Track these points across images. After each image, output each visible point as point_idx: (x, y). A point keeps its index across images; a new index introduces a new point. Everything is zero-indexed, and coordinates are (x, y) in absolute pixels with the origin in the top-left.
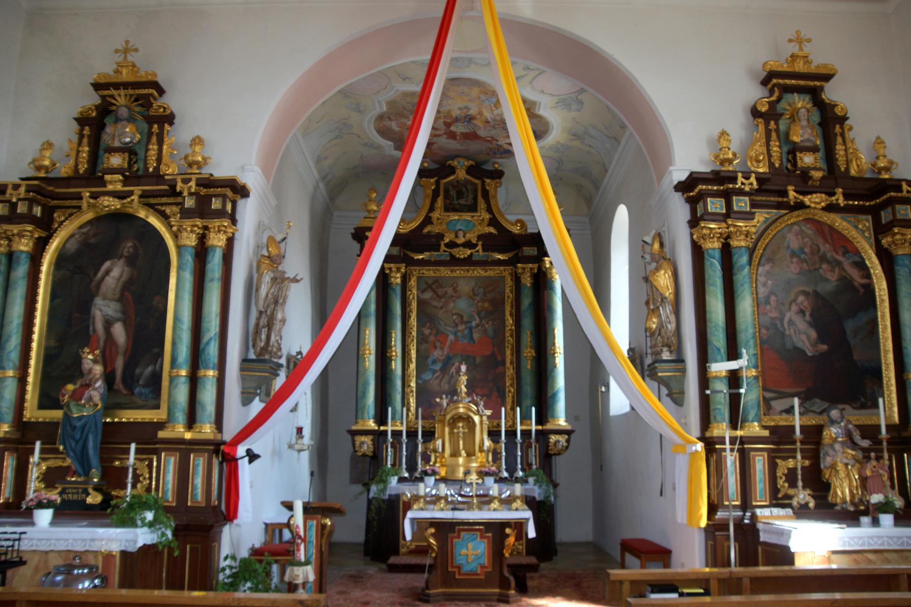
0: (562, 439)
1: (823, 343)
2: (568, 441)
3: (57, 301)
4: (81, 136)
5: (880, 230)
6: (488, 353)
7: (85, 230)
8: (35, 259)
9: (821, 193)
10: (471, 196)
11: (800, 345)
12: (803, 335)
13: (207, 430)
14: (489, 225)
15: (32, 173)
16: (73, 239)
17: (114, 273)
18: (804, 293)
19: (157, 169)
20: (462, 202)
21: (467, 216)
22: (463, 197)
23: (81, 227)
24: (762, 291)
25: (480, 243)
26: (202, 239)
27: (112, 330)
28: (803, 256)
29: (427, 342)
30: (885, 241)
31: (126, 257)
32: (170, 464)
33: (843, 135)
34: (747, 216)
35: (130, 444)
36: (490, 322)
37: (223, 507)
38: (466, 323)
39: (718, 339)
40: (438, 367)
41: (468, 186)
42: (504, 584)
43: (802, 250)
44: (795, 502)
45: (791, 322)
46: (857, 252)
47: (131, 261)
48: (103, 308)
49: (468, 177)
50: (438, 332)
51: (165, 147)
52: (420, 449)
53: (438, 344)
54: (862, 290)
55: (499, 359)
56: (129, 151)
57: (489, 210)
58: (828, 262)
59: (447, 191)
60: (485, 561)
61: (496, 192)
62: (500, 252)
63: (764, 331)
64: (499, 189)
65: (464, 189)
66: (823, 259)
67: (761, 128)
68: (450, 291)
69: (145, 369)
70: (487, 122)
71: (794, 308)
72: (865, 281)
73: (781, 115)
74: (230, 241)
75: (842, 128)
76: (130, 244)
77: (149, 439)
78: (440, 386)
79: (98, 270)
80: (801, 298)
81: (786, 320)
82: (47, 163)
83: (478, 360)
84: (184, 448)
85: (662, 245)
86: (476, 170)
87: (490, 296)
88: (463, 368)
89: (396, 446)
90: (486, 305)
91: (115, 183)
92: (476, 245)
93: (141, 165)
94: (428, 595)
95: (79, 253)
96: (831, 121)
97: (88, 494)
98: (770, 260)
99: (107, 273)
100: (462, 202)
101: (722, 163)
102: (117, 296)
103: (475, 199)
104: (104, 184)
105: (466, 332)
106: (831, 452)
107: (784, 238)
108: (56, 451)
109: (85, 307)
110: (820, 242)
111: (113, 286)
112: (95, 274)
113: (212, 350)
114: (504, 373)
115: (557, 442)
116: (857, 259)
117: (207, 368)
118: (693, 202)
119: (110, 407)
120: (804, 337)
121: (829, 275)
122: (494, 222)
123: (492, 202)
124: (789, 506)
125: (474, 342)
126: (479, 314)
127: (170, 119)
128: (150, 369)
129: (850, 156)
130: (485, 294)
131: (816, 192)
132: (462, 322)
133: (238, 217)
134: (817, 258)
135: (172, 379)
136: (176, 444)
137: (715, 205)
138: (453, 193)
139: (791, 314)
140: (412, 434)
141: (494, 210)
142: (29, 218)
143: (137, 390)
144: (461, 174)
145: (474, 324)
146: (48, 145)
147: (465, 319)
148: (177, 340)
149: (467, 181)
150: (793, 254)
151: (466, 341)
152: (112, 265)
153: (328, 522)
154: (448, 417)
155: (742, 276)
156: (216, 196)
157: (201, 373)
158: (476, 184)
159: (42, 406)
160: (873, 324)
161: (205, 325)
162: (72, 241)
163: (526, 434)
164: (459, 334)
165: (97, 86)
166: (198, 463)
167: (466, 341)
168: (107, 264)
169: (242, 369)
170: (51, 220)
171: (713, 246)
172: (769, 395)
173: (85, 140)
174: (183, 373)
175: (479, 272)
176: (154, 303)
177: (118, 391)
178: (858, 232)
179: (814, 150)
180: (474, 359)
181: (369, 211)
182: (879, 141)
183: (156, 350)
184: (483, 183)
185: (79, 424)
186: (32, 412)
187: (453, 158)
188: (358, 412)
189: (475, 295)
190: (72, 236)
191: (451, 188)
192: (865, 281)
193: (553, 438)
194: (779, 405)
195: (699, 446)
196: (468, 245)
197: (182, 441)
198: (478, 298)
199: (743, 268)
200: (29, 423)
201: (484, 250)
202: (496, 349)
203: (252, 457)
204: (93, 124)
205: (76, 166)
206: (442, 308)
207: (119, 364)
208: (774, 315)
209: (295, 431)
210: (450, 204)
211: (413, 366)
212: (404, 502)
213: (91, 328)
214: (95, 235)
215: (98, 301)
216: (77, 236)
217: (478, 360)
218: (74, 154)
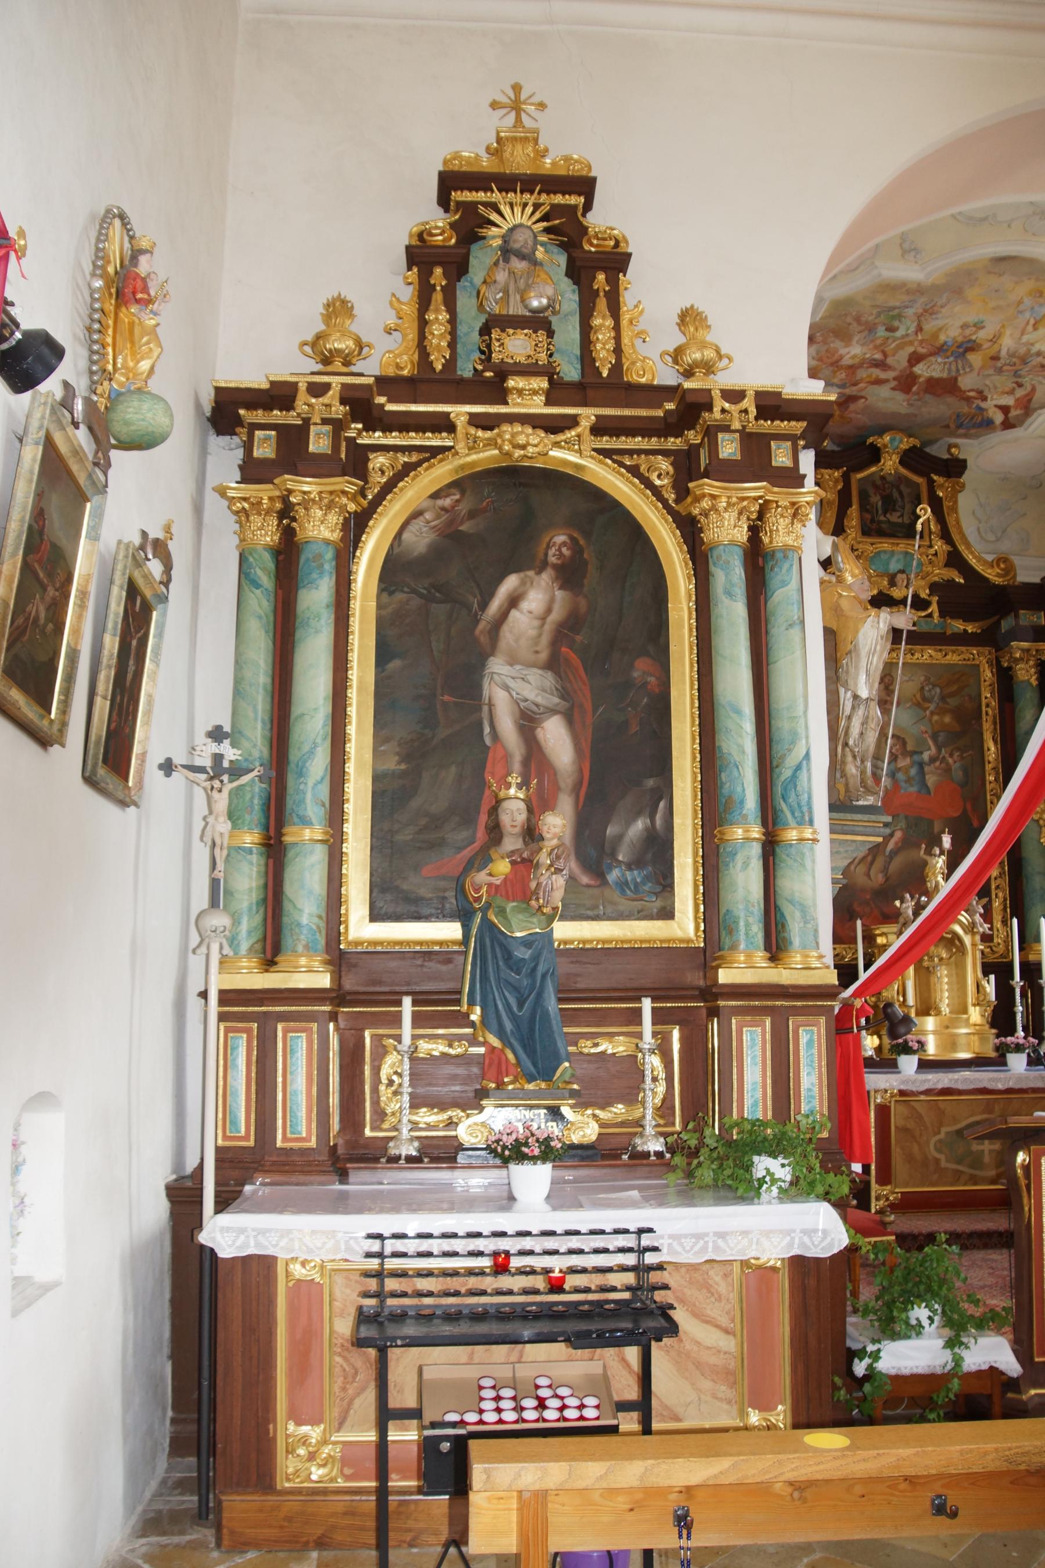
3: (395, 664)
6: (956, 814)
7: (447, 502)
14: (947, 565)
16: (419, 523)
17: (530, 605)
19: (617, 368)
20: (894, 518)
21: (902, 545)
22: (895, 510)
23: (435, 496)
25: (935, 599)
31: (555, 567)
32: (753, 1042)
35: (638, 1000)
36: (956, 754)
38: (913, 753)
41: (903, 488)
47: (569, 575)
48: (511, 683)
49: (903, 471)
57: (946, 535)
59: (864, 497)
61: (956, 502)
62: (966, 619)
64: (960, 495)
65: (896, 494)
69: (629, 823)
70: (995, 358)
76: (561, 539)
78: (868, 875)
79: (491, 595)
86: (915, 459)
87: (953, 702)
90: (947, 719)
91: (528, 397)
95: (437, 555)
99: (514, 601)
100: (894, 518)
102: (544, 656)
104: (501, 396)
105: (913, 772)
108: (463, 1019)
109: (465, 678)
111: (532, 633)
112: (484, 605)
122: (955, 560)
123: (951, 521)
125: (929, 793)
126: (934, 737)
128: (640, 825)
130: (943, 698)
132: (905, 753)
138: (876, 499)
141: (956, 537)
143: (614, 875)
144: (890, 464)
145: (926, 756)
147: (909, 748)
149: (900, 479)
151: (913, 789)
152: (523, 583)
158: (918, 485)
159: (376, 915)
162: (418, 524)
164: (900, 776)
167: (913, 789)
168: (511, 582)
175: (929, 654)
176: (636, 674)
184: (931, 483)
185: (522, 953)
186: (361, 928)
187: (881, 431)
189: (925, 699)
190: (417, 514)
191: (871, 491)
198: (932, 707)
201: (942, 615)
202: (969, 807)
210: (872, 521)
213: (487, 730)
214: (472, 515)
215: (497, 666)
216: (428, 516)
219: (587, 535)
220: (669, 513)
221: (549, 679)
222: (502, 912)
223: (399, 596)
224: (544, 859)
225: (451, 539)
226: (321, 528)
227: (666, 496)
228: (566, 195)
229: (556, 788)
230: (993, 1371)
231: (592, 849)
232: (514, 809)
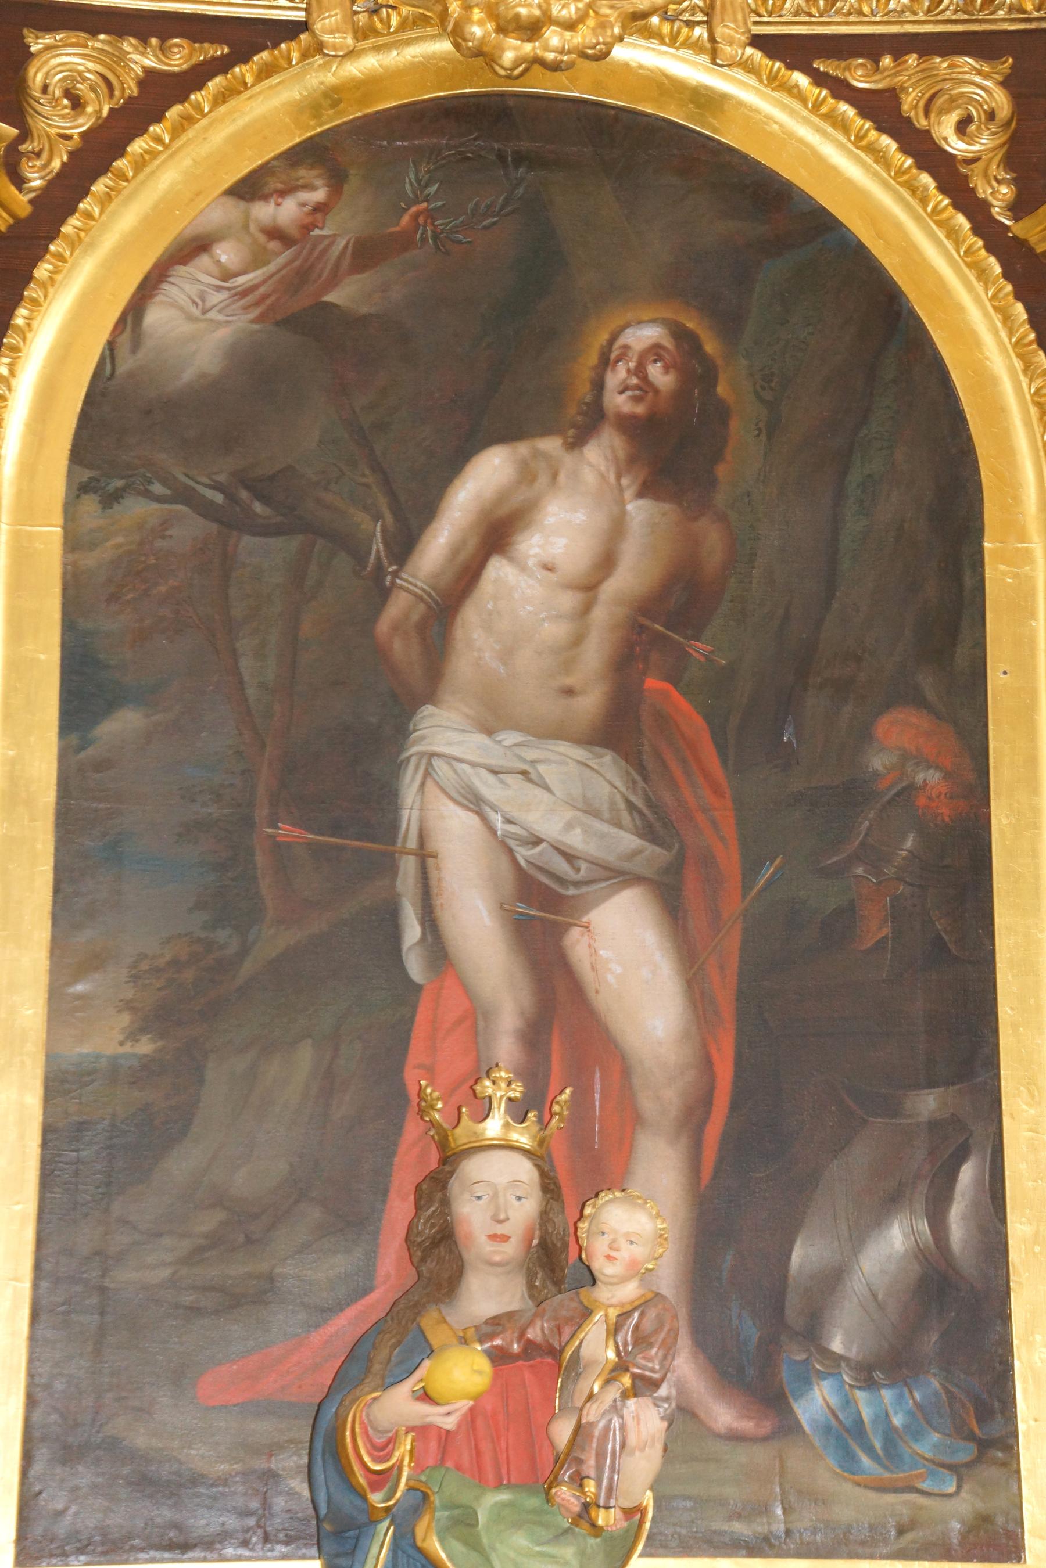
3: (123, 724)
7: (287, 211)
17: (550, 542)
23: (248, 189)
27: (577, 945)
31: (627, 425)
47: (671, 451)
48: (488, 787)
69: (857, 1240)
76: (644, 335)
79: (428, 510)
95: (256, 381)
99: (497, 533)
102: (591, 702)
111: (555, 631)
112: (405, 543)
128: (896, 1240)
143: (815, 1403)
152: (526, 474)
168: (488, 473)
176: (878, 762)
190: (192, 248)
213: (412, 932)
214: (366, 254)
215: (444, 733)
216: (226, 254)
219: (729, 324)
220: (990, 249)
221: (606, 776)
222: (463, 1524)
223: (137, 509)
224: (596, 1345)
225: (303, 332)
227: (983, 191)
229: (632, 1119)
231: (746, 1319)
232: (498, 1189)
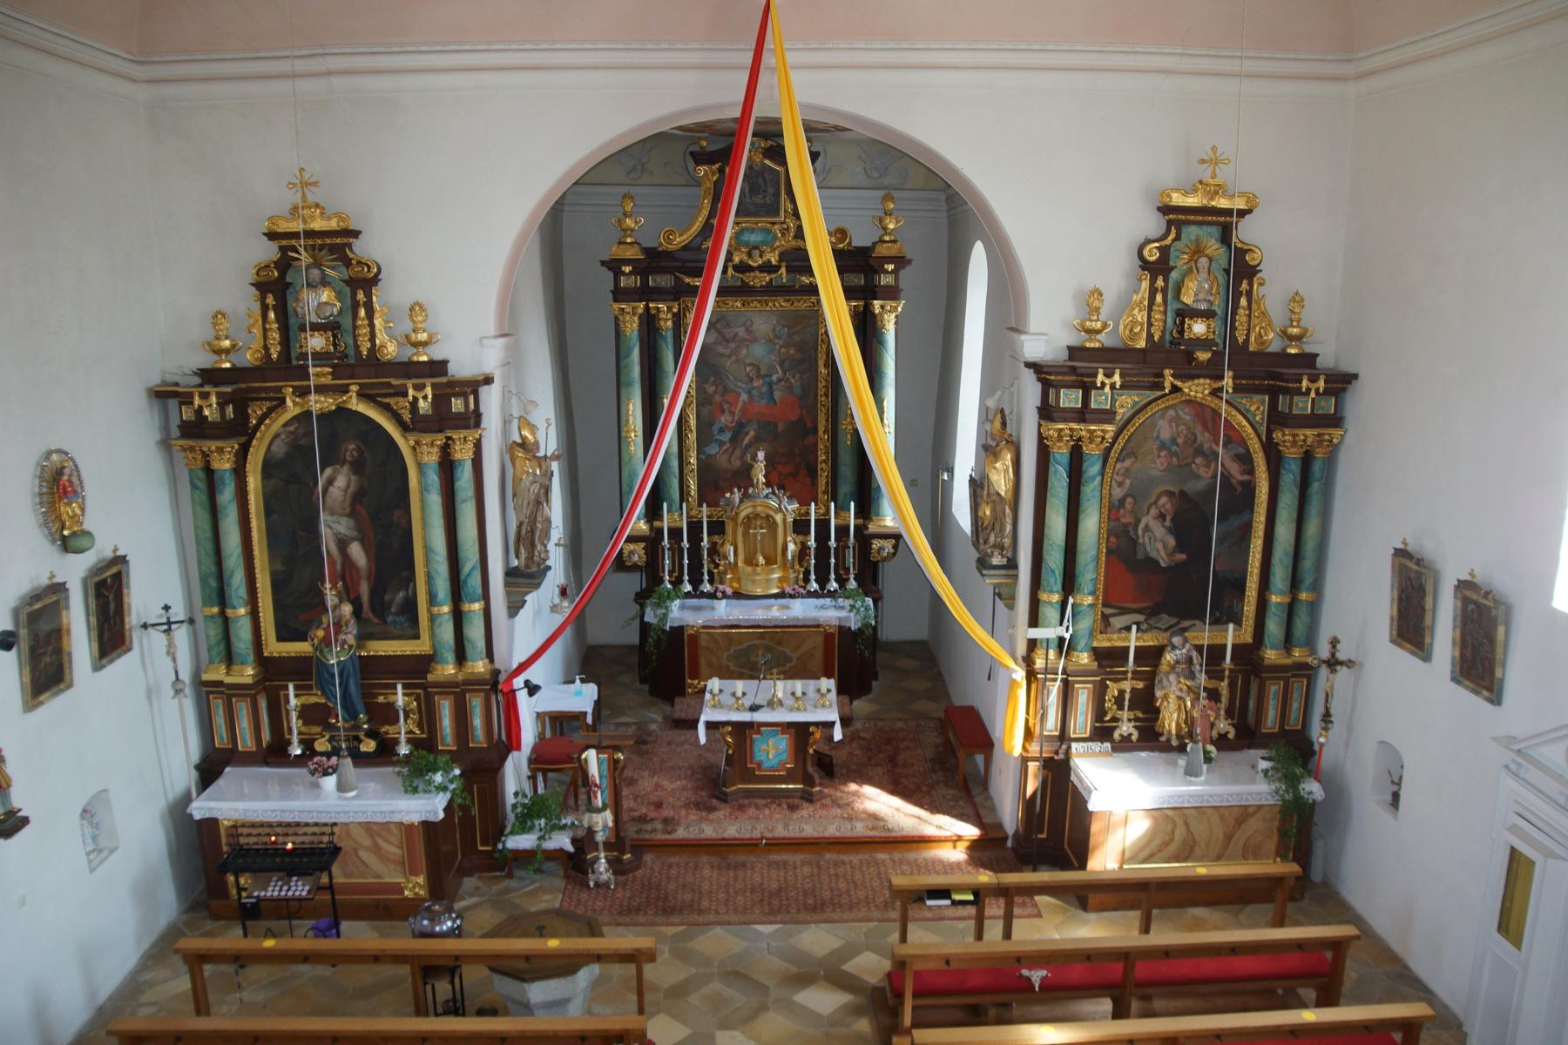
0: (888, 545)
1: (1181, 552)
2: (895, 547)
3: (275, 517)
4: (265, 309)
5: (1277, 419)
6: (794, 418)
7: (292, 428)
8: (240, 473)
9: (1205, 377)
10: (771, 191)
11: (1154, 555)
12: (1158, 542)
13: (479, 666)
15: (206, 360)
17: (337, 484)
18: (1170, 494)
21: (763, 222)
24: (1118, 492)
26: (446, 450)
28: (1174, 448)
29: (710, 403)
30: (1277, 436)
33: (1249, 294)
34: (1107, 416)
37: (504, 737)
38: (764, 377)
39: (1054, 560)
40: (726, 437)
42: (808, 781)
43: (1174, 441)
44: (1116, 735)
45: (1147, 529)
46: (1243, 442)
47: (357, 467)
50: (726, 390)
51: (378, 322)
52: (705, 543)
53: (726, 406)
54: (1239, 489)
55: (809, 425)
56: (330, 327)
58: (1204, 455)
60: (784, 757)
63: (1113, 539)
66: (1199, 451)
67: (1145, 285)
68: (741, 332)
71: (1154, 511)
72: (1246, 478)
73: (1173, 268)
74: (478, 445)
75: (1251, 285)
77: (416, 669)
80: (1164, 500)
81: (1142, 525)
82: (227, 343)
83: (780, 427)
84: (459, 691)
85: (1004, 424)
87: (797, 338)
88: (761, 455)
89: (677, 552)
92: (775, 269)
93: (351, 342)
94: (725, 794)
96: (1242, 270)
97: (360, 741)
98: (1133, 454)
101: (1088, 331)
103: (777, 195)
105: (764, 389)
106: (1165, 682)
107: (1155, 425)
110: (1199, 429)
113: (475, 582)
114: (816, 444)
115: (881, 549)
116: (1241, 450)
117: (472, 601)
118: (1046, 385)
119: (363, 638)
120: (1159, 546)
121: (1202, 471)
124: (1112, 741)
126: (782, 364)
127: (375, 280)
129: (1254, 321)
131: (1198, 377)
132: (759, 376)
133: (482, 409)
134: (1191, 451)
135: (432, 618)
136: (447, 687)
137: (1070, 399)
139: (1148, 520)
140: (695, 527)
142: (222, 431)
143: (390, 619)
145: (774, 378)
146: (219, 315)
148: (433, 574)
150: (1163, 446)
153: (621, 756)
154: (742, 515)
155: (1091, 492)
156: (457, 395)
157: (466, 607)
160: (1247, 528)
161: (462, 554)
162: (278, 442)
163: (842, 531)
164: (755, 392)
165: (272, 236)
166: (476, 704)
167: (764, 402)
169: (507, 584)
170: (247, 417)
171: (1061, 453)
172: (1108, 611)
173: (272, 315)
174: (446, 609)
175: (781, 303)
177: (368, 620)
178: (1246, 416)
179: (1208, 315)
180: (776, 425)
181: (624, 230)
182: (1297, 299)
183: (405, 574)
188: (623, 512)
190: (277, 436)
192: (1246, 478)
193: (876, 544)
194: (1118, 622)
195: (1020, 674)
196: (767, 268)
197: (456, 685)
199: (1093, 478)
200: (271, 659)
203: (533, 689)
204: (275, 287)
205: (266, 348)
206: (730, 356)
207: (364, 589)
208: (1127, 519)
209: (557, 591)
211: (692, 437)
212: (690, 636)
217: (780, 427)
218: (257, 331)
221: (351, 522)
223: (273, 481)
226: (224, 464)
228: (336, 245)
229: (359, 578)
230: (561, 850)
